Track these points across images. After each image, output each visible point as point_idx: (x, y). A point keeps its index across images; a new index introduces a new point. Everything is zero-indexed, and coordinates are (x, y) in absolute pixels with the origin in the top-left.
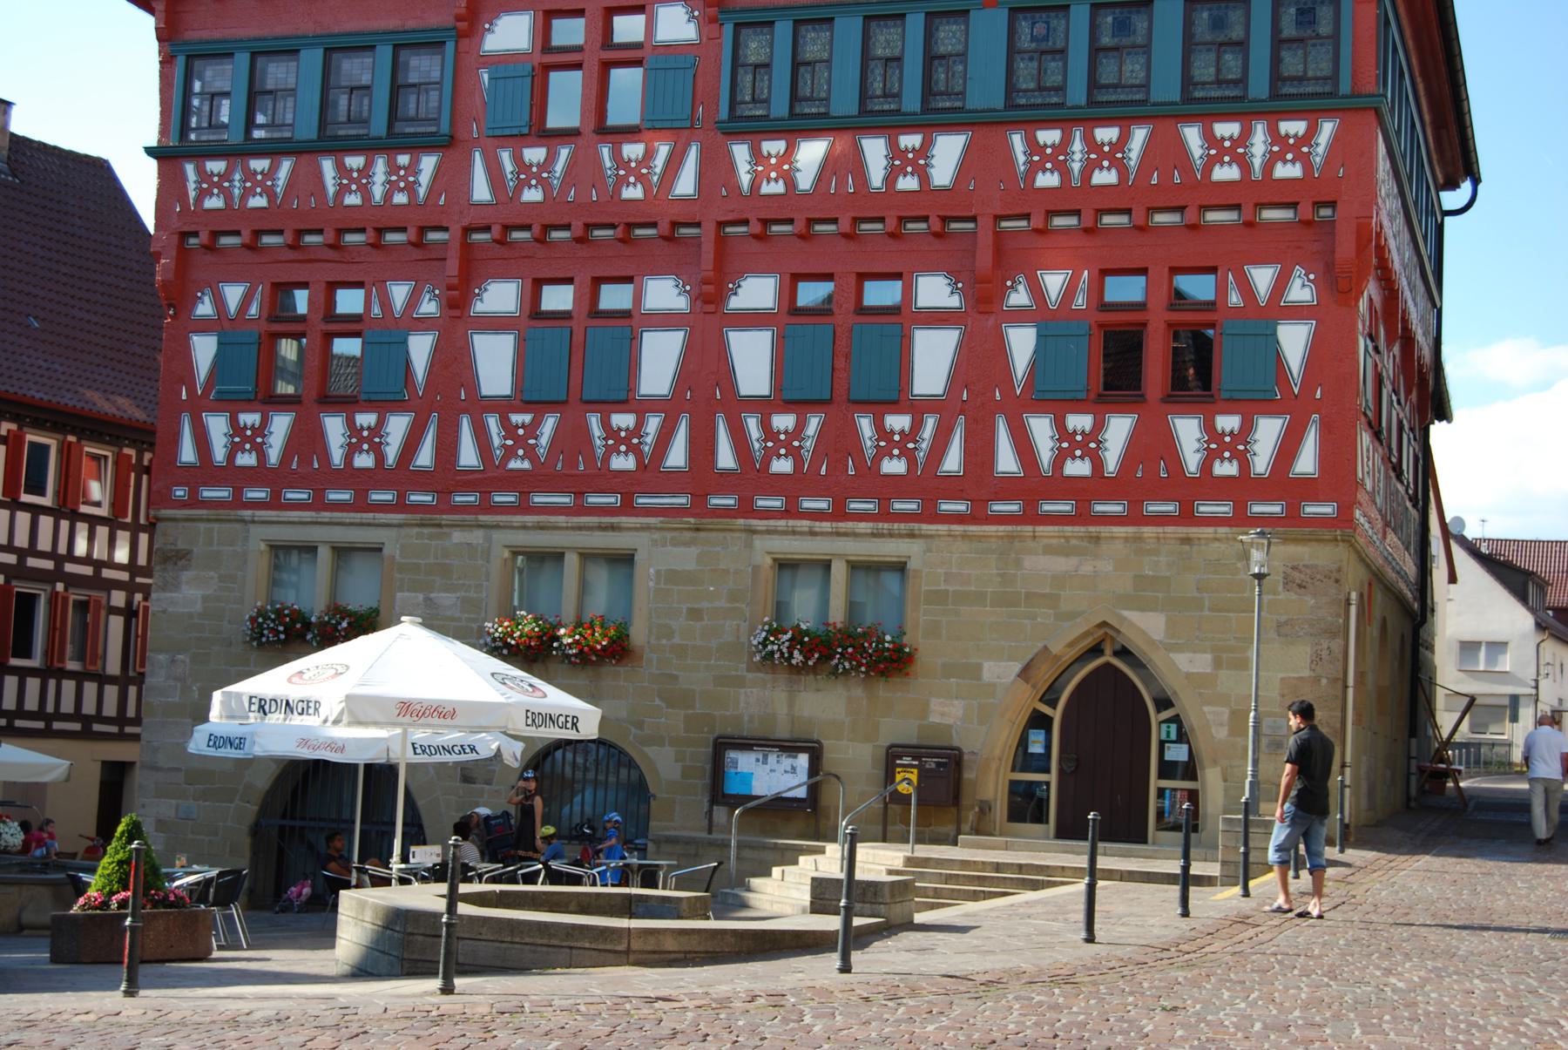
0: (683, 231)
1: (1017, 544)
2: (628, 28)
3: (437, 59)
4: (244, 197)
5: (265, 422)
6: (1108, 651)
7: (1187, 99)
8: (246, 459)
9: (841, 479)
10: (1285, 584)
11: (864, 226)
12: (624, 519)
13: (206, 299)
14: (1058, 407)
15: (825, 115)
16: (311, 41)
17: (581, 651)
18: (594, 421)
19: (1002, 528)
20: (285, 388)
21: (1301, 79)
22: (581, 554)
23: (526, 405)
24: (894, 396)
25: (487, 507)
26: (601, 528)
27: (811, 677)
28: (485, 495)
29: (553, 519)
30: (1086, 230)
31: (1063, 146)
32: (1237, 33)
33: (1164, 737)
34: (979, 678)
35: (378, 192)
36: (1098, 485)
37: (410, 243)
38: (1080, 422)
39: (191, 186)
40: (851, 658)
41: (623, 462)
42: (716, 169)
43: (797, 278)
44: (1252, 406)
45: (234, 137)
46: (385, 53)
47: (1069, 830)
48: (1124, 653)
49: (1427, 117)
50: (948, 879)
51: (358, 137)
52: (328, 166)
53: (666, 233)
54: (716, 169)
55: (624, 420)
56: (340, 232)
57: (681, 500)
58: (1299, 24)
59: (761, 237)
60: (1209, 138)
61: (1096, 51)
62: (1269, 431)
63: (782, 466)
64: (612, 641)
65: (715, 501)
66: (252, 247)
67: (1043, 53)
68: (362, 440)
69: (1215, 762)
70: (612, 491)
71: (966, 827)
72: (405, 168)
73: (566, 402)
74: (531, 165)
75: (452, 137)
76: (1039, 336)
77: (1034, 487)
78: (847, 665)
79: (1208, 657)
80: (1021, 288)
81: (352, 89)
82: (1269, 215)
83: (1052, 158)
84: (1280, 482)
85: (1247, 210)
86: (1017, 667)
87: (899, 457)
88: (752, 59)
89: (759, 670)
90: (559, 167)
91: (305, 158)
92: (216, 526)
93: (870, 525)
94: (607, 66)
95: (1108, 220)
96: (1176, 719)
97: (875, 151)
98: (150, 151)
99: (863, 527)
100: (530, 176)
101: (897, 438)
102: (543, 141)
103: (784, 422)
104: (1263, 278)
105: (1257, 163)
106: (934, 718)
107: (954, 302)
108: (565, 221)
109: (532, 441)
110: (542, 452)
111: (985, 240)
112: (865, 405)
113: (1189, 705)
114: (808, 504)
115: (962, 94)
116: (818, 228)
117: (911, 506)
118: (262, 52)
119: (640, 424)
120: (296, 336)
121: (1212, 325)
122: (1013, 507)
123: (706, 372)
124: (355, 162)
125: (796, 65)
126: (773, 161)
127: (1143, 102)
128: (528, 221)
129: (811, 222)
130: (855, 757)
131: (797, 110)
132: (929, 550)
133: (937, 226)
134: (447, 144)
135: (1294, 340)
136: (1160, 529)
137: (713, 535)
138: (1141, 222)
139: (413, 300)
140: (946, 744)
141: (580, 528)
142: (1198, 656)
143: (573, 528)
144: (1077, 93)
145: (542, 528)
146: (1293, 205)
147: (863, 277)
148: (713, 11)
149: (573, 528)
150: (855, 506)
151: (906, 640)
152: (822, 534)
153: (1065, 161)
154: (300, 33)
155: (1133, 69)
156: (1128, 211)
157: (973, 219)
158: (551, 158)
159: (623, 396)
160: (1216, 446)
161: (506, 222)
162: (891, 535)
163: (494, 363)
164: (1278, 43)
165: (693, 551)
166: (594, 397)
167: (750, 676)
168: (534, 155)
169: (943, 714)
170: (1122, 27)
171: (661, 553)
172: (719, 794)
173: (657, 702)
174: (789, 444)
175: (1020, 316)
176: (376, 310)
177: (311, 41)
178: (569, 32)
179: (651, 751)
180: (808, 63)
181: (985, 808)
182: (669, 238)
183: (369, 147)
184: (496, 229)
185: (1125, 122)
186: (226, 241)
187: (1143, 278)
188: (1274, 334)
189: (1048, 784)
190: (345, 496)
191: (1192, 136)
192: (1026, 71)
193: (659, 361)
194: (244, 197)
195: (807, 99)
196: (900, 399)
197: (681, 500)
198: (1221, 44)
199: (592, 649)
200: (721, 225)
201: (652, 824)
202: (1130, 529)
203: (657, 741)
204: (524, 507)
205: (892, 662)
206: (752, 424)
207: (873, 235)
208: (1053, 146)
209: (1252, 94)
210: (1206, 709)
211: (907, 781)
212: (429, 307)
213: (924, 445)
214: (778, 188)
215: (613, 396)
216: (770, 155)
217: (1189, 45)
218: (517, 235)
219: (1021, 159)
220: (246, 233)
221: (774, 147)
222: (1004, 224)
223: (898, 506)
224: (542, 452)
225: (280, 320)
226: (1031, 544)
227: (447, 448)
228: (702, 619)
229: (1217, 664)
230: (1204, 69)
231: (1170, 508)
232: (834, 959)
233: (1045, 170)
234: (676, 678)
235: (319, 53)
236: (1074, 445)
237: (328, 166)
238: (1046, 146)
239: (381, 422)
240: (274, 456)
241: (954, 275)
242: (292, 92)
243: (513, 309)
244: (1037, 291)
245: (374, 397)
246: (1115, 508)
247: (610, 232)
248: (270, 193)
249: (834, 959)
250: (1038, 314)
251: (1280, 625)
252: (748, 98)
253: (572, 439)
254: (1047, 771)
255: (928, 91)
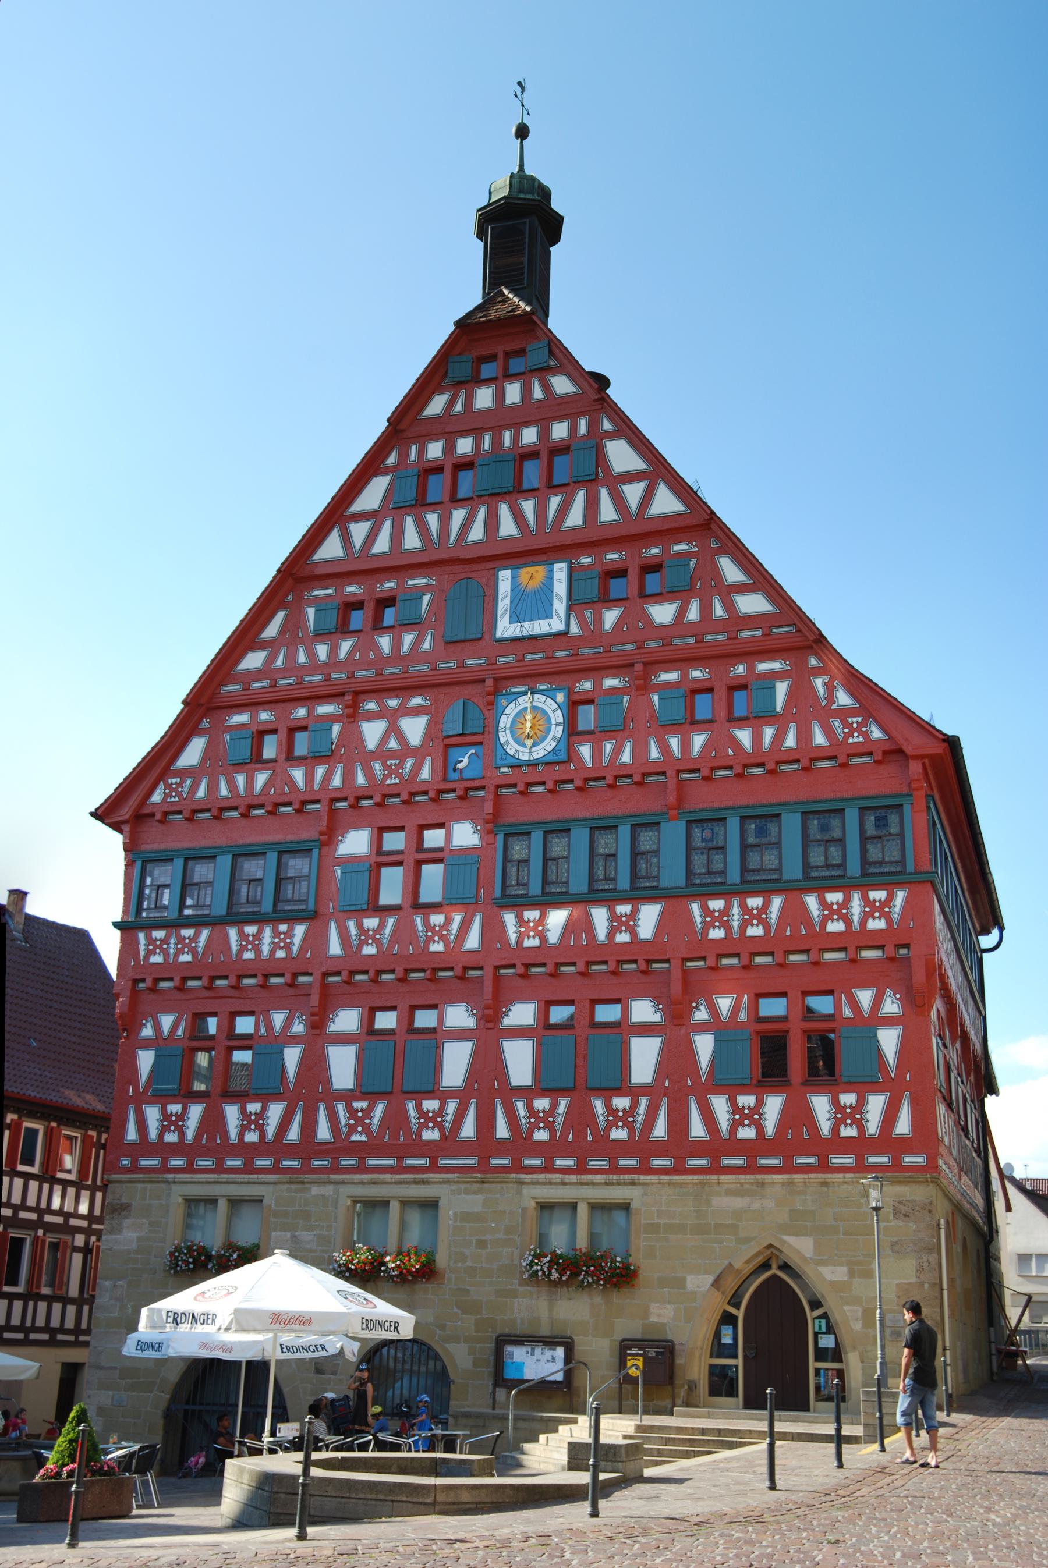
0: (472, 973)
1: (707, 1188)
2: (433, 838)
3: (307, 860)
4: (176, 955)
5: (185, 1110)
6: (774, 1266)
7: (807, 877)
8: (171, 1137)
9: (583, 1144)
10: (895, 1214)
11: (594, 967)
12: (431, 1175)
13: (149, 1025)
14: (731, 1090)
15: (566, 893)
16: (223, 850)
17: (401, 1273)
18: (411, 1106)
19: (696, 1177)
20: (199, 1086)
21: (881, 863)
22: (401, 1202)
23: (364, 1095)
24: (618, 1085)
25: (336, 1169)
26: (416, 1182)
27: (565, 1289)
28: (335, 1159)
29: (382, 1176)
30: (744, 967)
31: (726, 911)
32: (837, 834)
33: (817, 1329)
34: (684, 1287)
35: (266, 950)
36: (761, 1145)
37: (286, 984)
38: (747, 1100)
39: (142, 948)
40: (593, 1274)
41: (431, 1135)
42: (493, 930)
43: (549, 1003)
44: (864, 1087)
45: (172, 914)
46: (272, 856)
47: (754, 1402)
48: (785, 1267)
49: (965, 886)
50: (668, 1441)
51: (254, 913)
52: (233, 933)
53: (460, 974)
54: (493, 930)
55: (431, 1105)
56: (240, 977)
57: (472, 1161)
58: (877, 826)
59: (524, 976)
60: (823, 903)
61: (745, 848)
62: (876, 1104)
63: (541, 1135)
64: (423, 1265)
65: (495, 1161)
66: (181, 989)
67: (710, 849)
68: (250, 1122)
69: (854, 1348)
70: (423, 1156)
71: (679, 1401)
72: (284, 933)
73: (391, 1093)
74: (369, 930)
75: (316, 912)
76: (716, 1040)
77: (717, 1147)
78: (590, 1279)
79: (845, 1269)
80: (702, 1008)
81: (250, 881)
82: (866, 954)
83: (719, 919)
84: (886, 1140)
85: (851, 950)
86: (710, 1279)
87: (622, 1127)
88: (516, 857)
89: (528, 1285)
90: (388, 931)
91: (218, 927)
92: (149, 1186)
93: (604, 1176)
94: (419, 863)
95: (759, 960)
96: (825, 1316)
97: (600, 916)
98: (116, 925)
99: (599, 1178)
100: (368, 937)
101: (621, 1114)
102: (377, 913)
103: (542, 1104)
104: (865, 997)
105: (856, 919)
106: (653, 1319)
107: (657, 1018)
108: (391, 967)
109: (367, 1121)
110: (374, 1128)
111: (676, 975)
112: (598, 1091)
113: (832, 1304)
114: (560, 1162)
115: (657, 878)
116: (563, 969)
117: (632, 1162)
118: (192, 858)
119: (443, 1107)
120: (208, 1050)
121: (833, 1031)
122: (703, 1162)
123: (487, 1067)
124: (251, 930)
125: (546, 860)
126: (532, 924)
127: (778, 880)
128: (366, 968)
129: (558, 965)
130: (597, 1348)
131: (547, 890)
132: (646, 1195)
133: (643, 967)
134: (313, 916)
135: (889, 1040)
136: (806, 1176)
137: (494, 1185)
138: (780, 961)
139: (288, 1023)
140: (662, 1337)
141: (401, 1183)
142: (838, 1268)
143: (396, 1183)
144: (734, 875)
145: (374, 1183)
146: (881, 947)
147: (594, 1002)
148: (490, 826)
149: (396, 1183)
150: (593, 1163)
151: (631, 1260)
152: (570, 1184)
153: (728, 920)
154: (217, 845)
155: (770, 859)
156: (772, 954)
157: (668, 961)
158: (382, 925)
159: (430, 1088)
160: (841, 1115)
161: (352, 969)
162: (619, 1184)
163: (342, 1066)
164: (864, 839)
165: (480, 1198)
166: (410, 1089)
167: (521, 1289)
168: (371, 923)
169: (659, 1315)
170: (761, 831)
171: (458, 1200)
172: (500, 1380)
173: (455, 1310)
174: (545, 1119)
175: (702, 1027)
176: (263, 1031)
177: (223, 850)
178: (395, 841)
179: (451, 1347)
180: (554, 859)
181: (692, 1386)
182: (462, 978)
183: (260, 920)
184: (345, 974)
185: (767, 894)
186: (163, 985)
187: (784, 1000)
188: (875, 1036)
189: (736, 1367)
190: (237, 1162)
191: (811, 902)
192: (699, 861)
193: (456, 1063)
194: (176, 955)
195: (553, 883)
196: (623, 1087)
197: (472, 1161)
198: (827, 841)
199: (409, 1271)
200: (497, 968)
201: (452, 1402)
202: (786, 1176)
203: (455, 1339)
204: (362, 1169)
205: (621, 1277)
206: (520, 1106)
207: (600, 973)
208: (719, 911)
209: (849, 874)
210: (845, 1308)
211: (635, 1367)
212: (298, 1028)
213: (640, 1119)
214: (535, 942)
215: (424, 1088)
216: (529, 921)
217: (806, 842)
218: (359, 977)
219: (698, 920)
220: (177, 979)
221: (532, 915)
222: (689, 964)
223: (623, 1163)
224: (374, 1128)
225: (198, 1039)
226: (717, 1188)
227: (309, 1127)
228: (486, 1247)
229: (851, 1274)
230: (817, 857)
231: (811, 1160)
232: (586, 1507)
233: (714, 927)
234: (468, 1291)
235: (230, 857)
236: (744, 1117)
237: (233, 933)
238: (714, 911)
239: (264, 1109)
240: (190, 1134)
241: (656, 999)
242: (211, 884)
243: (355, 1028)
244: (713, 1009)
245: (259, 1092)
246: (774, 1161)
247: (421, 975)
248: (194, 952)
249: (586, 1507)
250: (715, 1025)
251: (893, 1245)
252: (514, 883)
253: (396, 1119)
254: (736, 1357)
255: (634, 875)
